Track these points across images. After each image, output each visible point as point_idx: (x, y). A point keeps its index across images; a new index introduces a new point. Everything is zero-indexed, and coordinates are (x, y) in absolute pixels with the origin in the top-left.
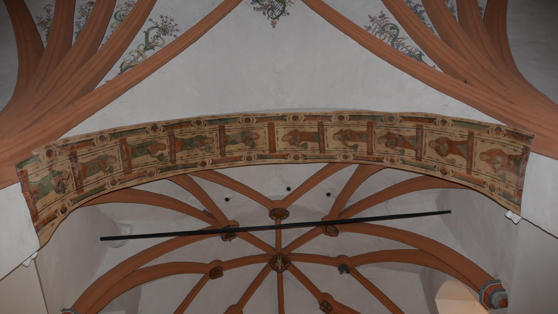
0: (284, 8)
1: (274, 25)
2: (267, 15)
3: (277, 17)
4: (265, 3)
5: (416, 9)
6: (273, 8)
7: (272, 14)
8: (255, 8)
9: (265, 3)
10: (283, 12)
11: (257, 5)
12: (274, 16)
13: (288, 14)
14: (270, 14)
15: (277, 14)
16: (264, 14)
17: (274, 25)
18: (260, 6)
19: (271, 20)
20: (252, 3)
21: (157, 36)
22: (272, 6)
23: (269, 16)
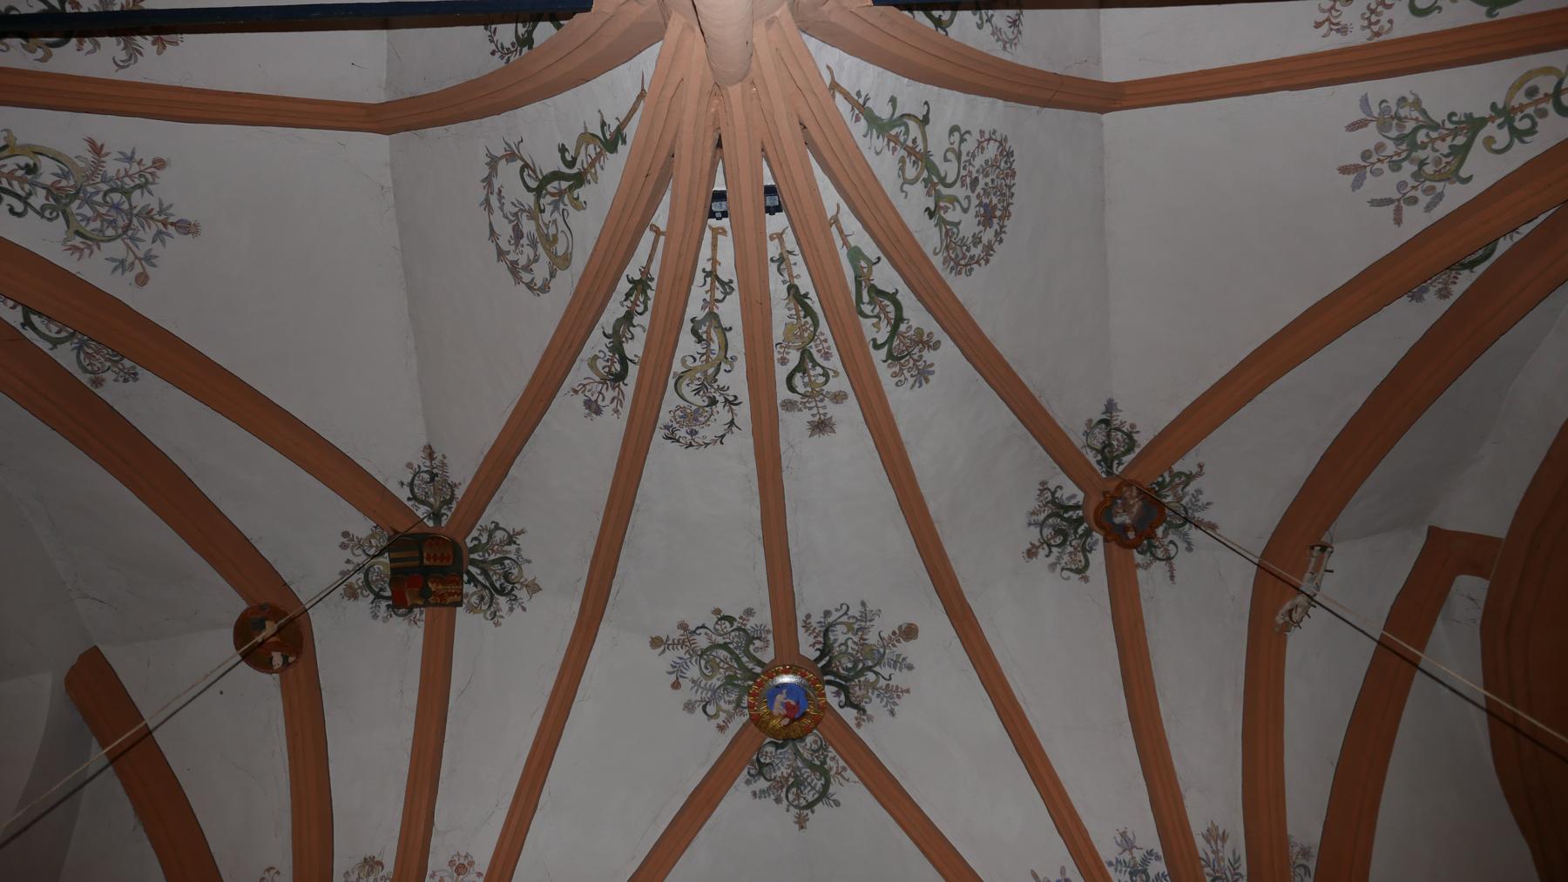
0: (826, 786)
1: (801, 823)
2: (785, 802)
3: (810, 806)
4: (779, 773)
5: (1144, 871)
6: (799, 783)
7: (798, 796)
8: (754, 794)
9: (779, 773)
10: (823, 794)
11: (762, 784)
12: (804, 803)
13: (837, 804)
14: (791, 797)
15: (810, 799)
16: (778, 800)
17: (801, 823)
18: (767, 784)
19: (794, 811)
20: (748, 782)
22: (796, 777)
23: (790, 804)
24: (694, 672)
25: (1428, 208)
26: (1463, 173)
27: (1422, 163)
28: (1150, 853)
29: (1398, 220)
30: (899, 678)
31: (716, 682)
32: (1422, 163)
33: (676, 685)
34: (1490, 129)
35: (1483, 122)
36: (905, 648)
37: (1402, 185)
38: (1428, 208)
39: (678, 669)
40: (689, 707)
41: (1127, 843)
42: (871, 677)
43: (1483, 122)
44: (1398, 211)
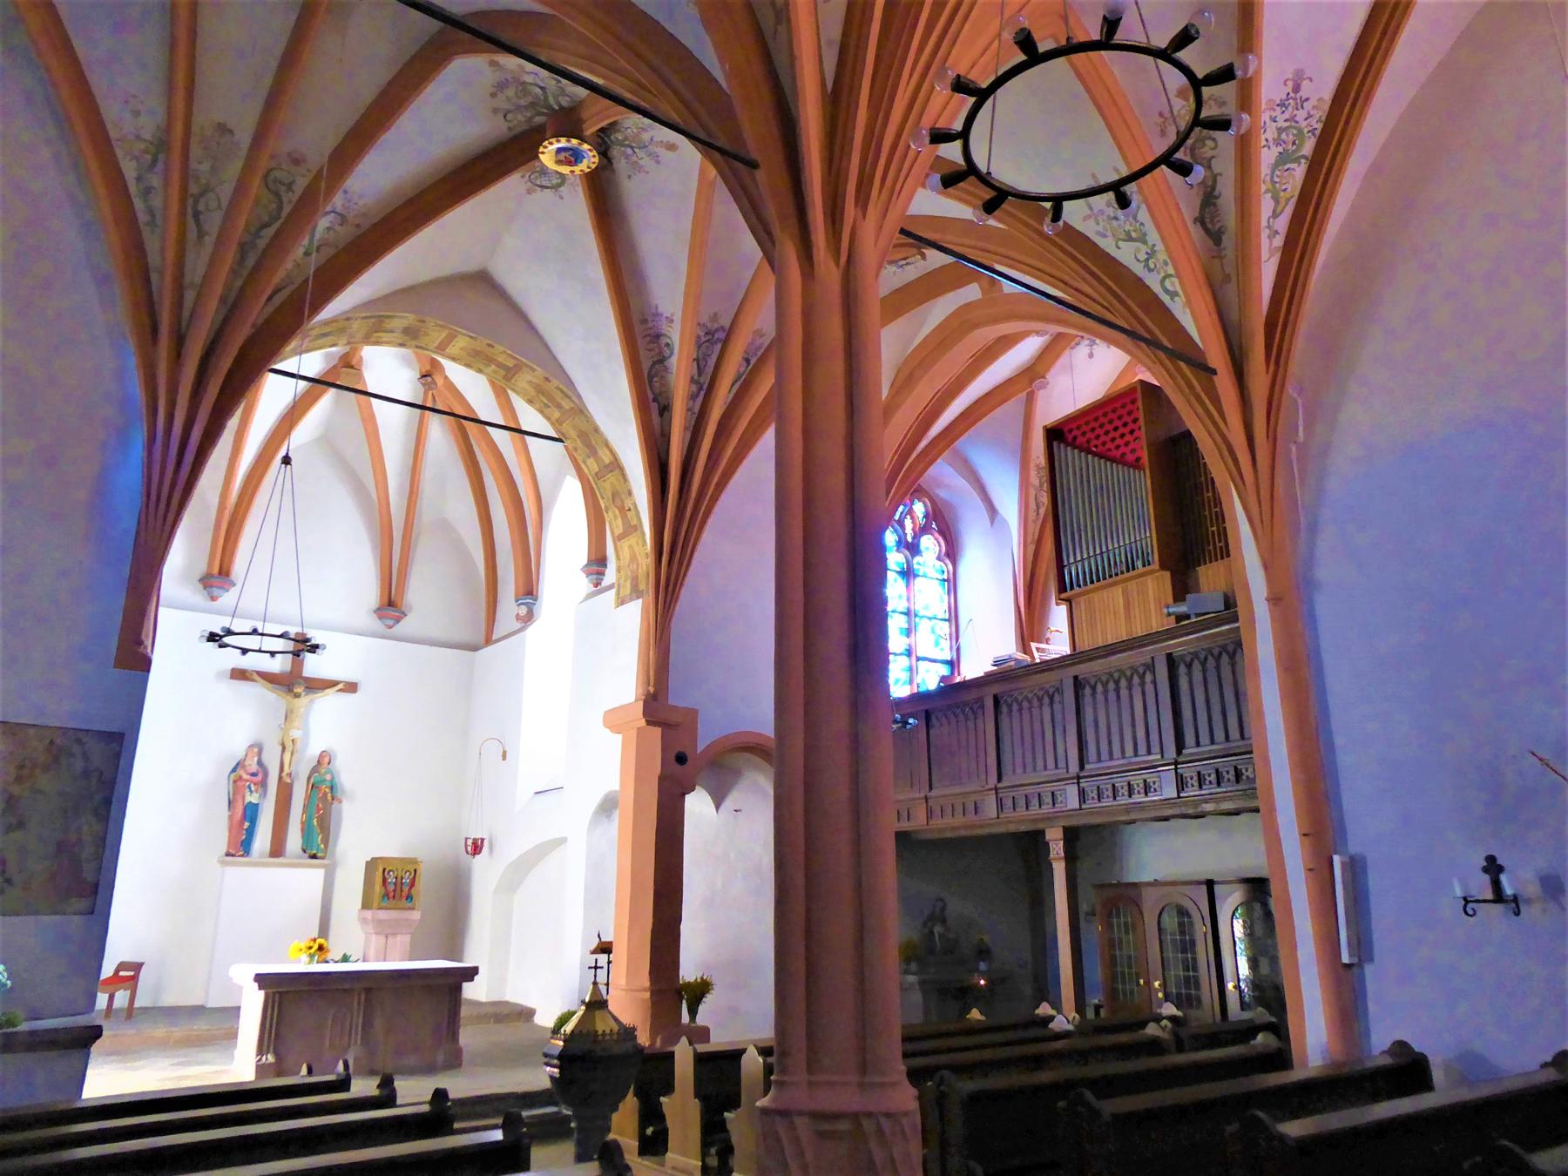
3: (543, 187)
21: (329, 229)
24: (510, 92)
25: (1098, 233)
26: (1121, 244)
27: (1116, 218)
28: (722, 328)
29: (1085, 219)
30: (646, 162)
31: (523, 102)
32: (1116, 218)
33: (493, 95)
34: (1144, 248)
35: (1145, 242)
36: (661, 151)
37: (1102, 212)
38: (1098, 233)
39: (501, 86)
40: (495, 111)
41: (715, 317)
42: (629, 151)
43: (1145, 242)
44: (1089, 217)
